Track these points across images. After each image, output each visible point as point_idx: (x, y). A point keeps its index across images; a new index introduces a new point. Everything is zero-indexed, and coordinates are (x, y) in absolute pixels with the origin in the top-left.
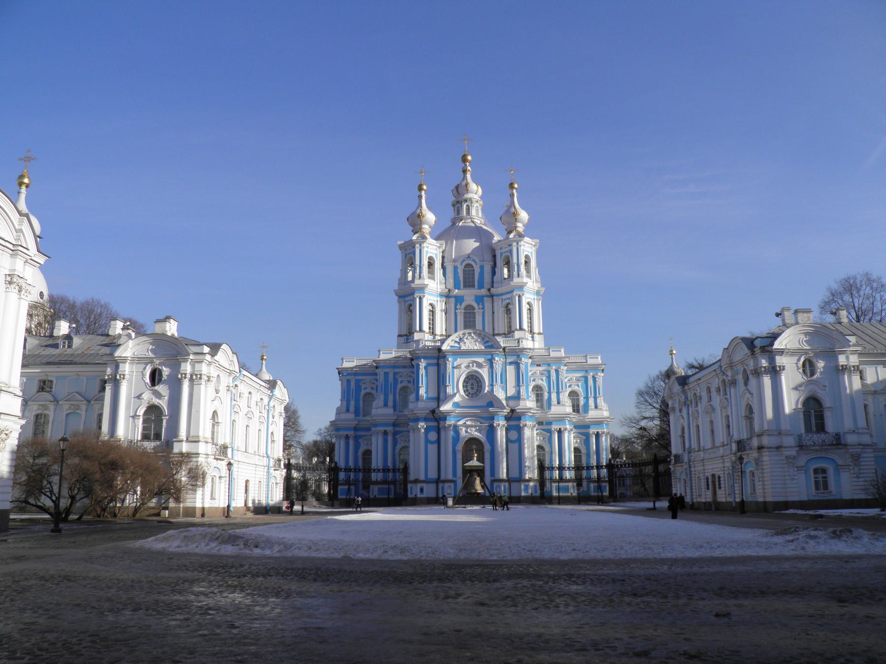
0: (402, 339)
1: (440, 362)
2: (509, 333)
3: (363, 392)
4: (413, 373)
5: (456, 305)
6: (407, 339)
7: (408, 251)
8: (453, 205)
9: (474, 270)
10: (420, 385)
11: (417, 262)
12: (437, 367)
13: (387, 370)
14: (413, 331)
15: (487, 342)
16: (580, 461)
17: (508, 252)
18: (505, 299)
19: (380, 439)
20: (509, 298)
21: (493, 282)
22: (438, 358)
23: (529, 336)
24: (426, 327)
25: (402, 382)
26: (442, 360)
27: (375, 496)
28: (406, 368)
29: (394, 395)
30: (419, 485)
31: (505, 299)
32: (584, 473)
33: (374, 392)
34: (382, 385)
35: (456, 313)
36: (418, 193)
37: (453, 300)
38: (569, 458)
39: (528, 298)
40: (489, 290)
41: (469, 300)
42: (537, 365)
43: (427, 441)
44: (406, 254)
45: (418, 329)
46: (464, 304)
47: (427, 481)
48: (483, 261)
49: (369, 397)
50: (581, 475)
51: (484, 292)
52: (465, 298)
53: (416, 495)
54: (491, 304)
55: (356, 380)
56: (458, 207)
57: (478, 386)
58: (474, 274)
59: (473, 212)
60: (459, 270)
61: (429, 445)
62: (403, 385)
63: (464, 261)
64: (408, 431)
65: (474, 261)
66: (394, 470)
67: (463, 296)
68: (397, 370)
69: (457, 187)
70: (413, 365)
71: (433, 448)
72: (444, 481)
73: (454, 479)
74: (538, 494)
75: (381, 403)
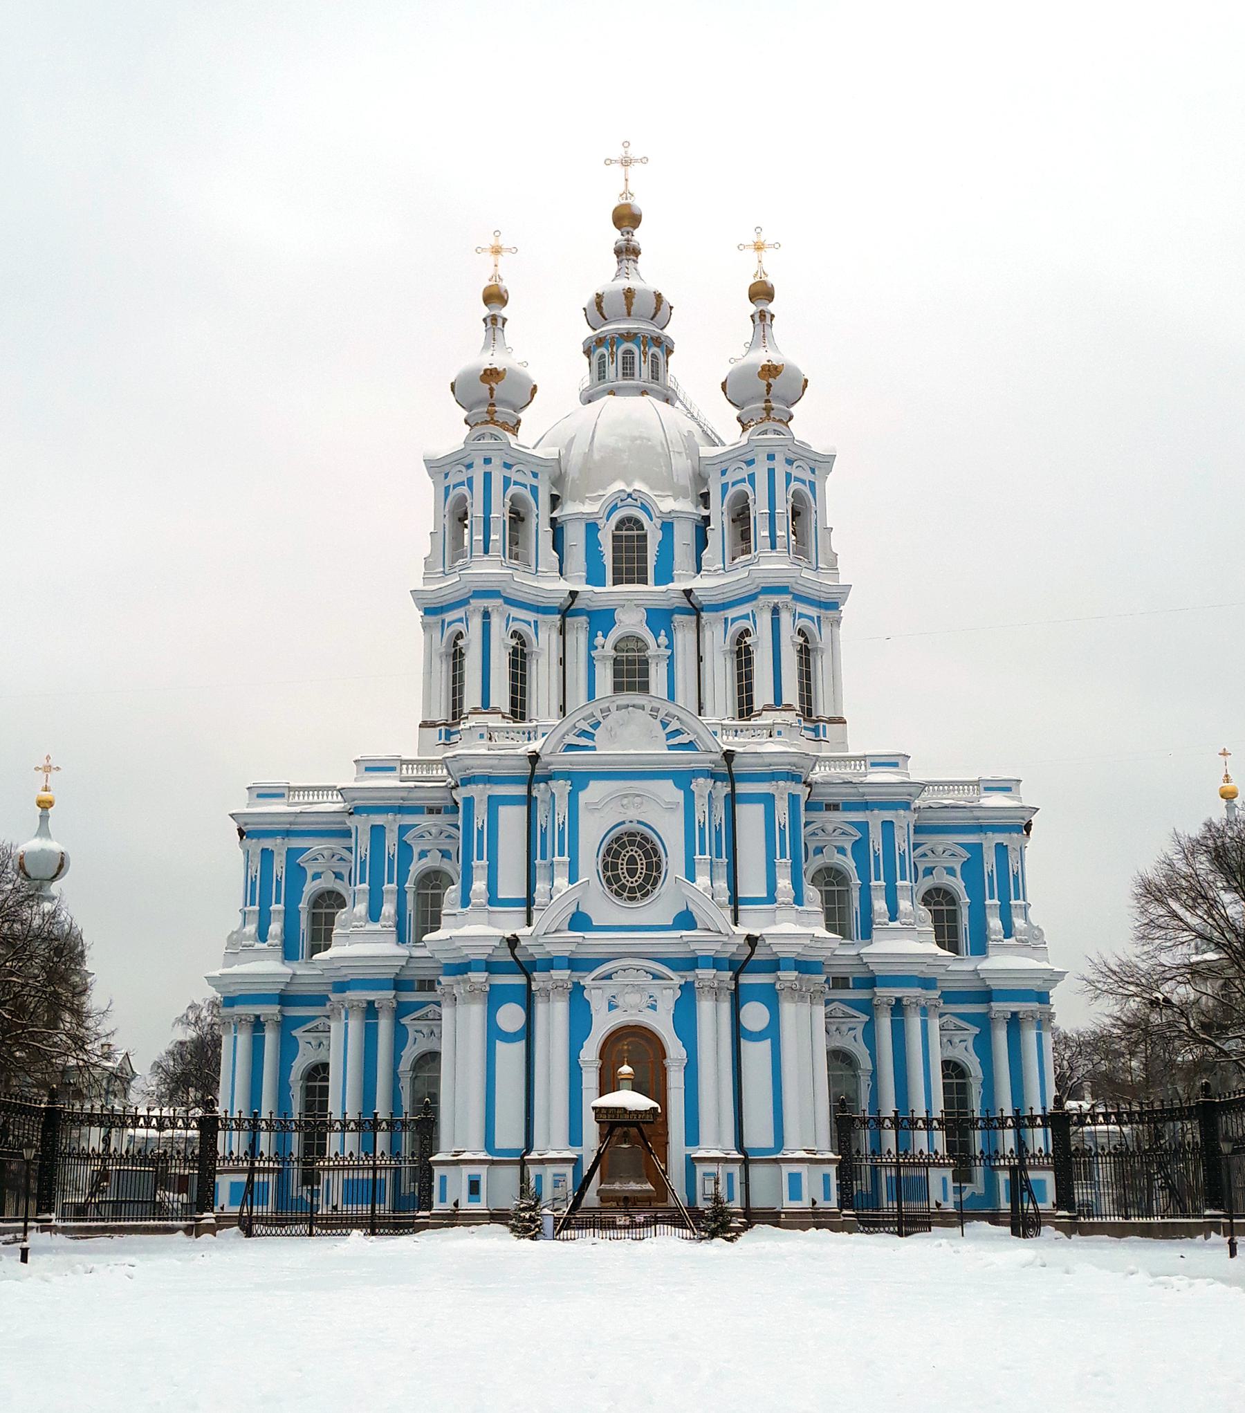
1: (534, 794)
5: (592, 637)
6: (449, 734)
7: (452, 480)
8: (588, 352)
10: (475, 863)
12: (525, 808)
13: (378, 820)
14: (466, 709)
15: (677, 732)
16: (964, 1102)
17: (743, 480)
18: (734, 620)
19: (355, 1025)
20: (746, 617)
22: (531, 780)
24: (501, 697)
26: (542, 785)
27: (335, 1208)
28: (439, 812)
29: (401, 894)
30: (467, 1171)
31: (734, 620)
32: (978, 1139)
33: (339, 886)
34: (363, 863)
37: (578, 624)
39: (801, 615)
41: (631, 622)
43: (494, 1034)
44: (447, 488)
49: (329, 902)
50: (966, 1146)
52: (619, 615)
53: (456, 1204)
56: (603, 356)
57: (649, 866)
64: (438, 1004)
65: (644, 508)
66: (393, 1125)
68: (408, 820)
69: (599, 297)
70: (456, 803)
71: (510, 1055)
74: (833, 1204)
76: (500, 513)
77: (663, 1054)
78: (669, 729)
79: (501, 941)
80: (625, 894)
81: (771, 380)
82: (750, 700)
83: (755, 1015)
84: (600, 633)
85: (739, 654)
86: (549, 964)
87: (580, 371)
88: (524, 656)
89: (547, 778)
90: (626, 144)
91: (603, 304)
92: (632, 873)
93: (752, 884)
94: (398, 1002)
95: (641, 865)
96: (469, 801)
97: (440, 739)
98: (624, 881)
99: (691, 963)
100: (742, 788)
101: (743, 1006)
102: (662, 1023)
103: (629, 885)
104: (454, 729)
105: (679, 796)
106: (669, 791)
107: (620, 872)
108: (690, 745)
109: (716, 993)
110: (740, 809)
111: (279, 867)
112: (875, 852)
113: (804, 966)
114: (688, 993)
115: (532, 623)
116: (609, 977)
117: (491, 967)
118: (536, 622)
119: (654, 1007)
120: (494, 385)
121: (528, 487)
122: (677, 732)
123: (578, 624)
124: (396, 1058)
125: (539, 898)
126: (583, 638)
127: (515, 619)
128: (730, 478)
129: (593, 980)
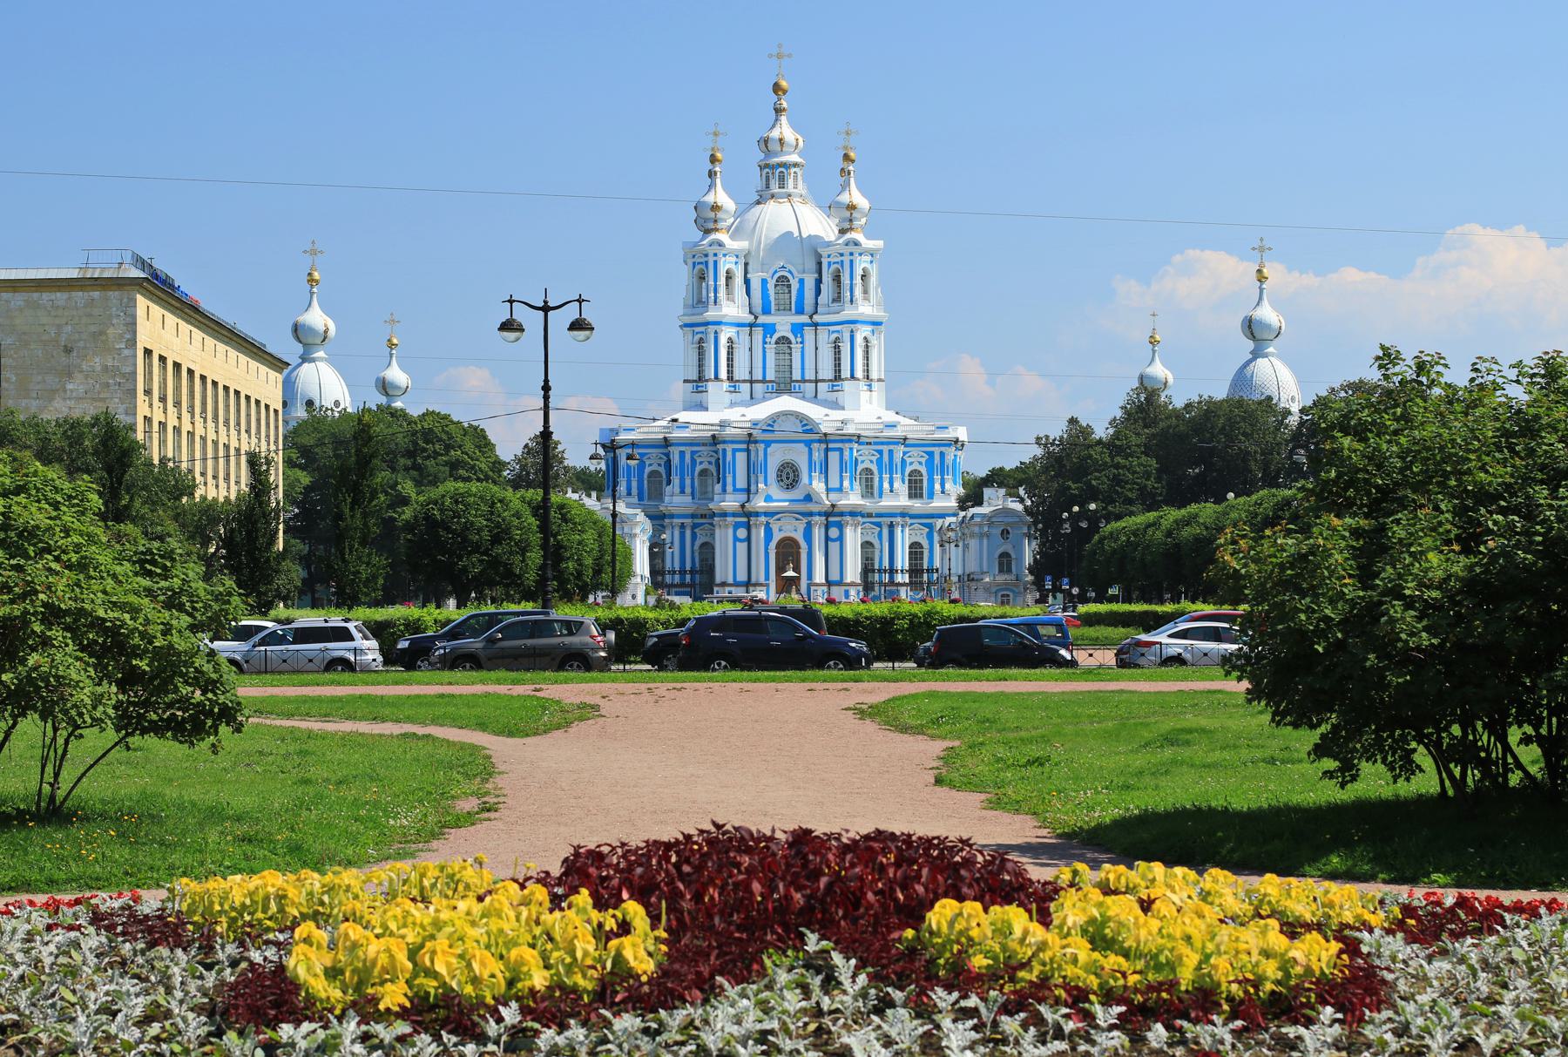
0: (690, 385)
2: (838, 377)
3: (647, 470)
5: (765, 337)
9: (789, 286)
11: (711, 283)
21: (817, 303)
22: (749, 443)
23: (862, 385)
24: (723, 374)
25: (701, 463)
29: (693, 479)
35: (764, 348)
36: (710, 166)
37: (758, 334)
38: (902, 560)
40: (811, 317)
41: (784, 330)
43: (736, 539)
46: (776, 336)
47: (736, 584)
48: (804, 272)
51: (804, 319)
52: (777, 327)
59: (791, 182)
62: (702, 467)
65: (790, 272)
66: (692, 572)
71: (742, 547)
75: (677, 490)
76: (722, 281)
83: (834, 533)
86: (757, 514)
87: (756, 181)
89: (756, 442)
90: (780, 46)
93: (834, 483)
95: (791, 475)
96: (724, 450)
99: (811, 514)
100: (831, 446)
102: (799, 537)
108: (810, 431)
113: (853, 514)
114: (809, 527)
117: (734, 515)
123: (758, 334)
125: (753, 488)
126: (760, 337)
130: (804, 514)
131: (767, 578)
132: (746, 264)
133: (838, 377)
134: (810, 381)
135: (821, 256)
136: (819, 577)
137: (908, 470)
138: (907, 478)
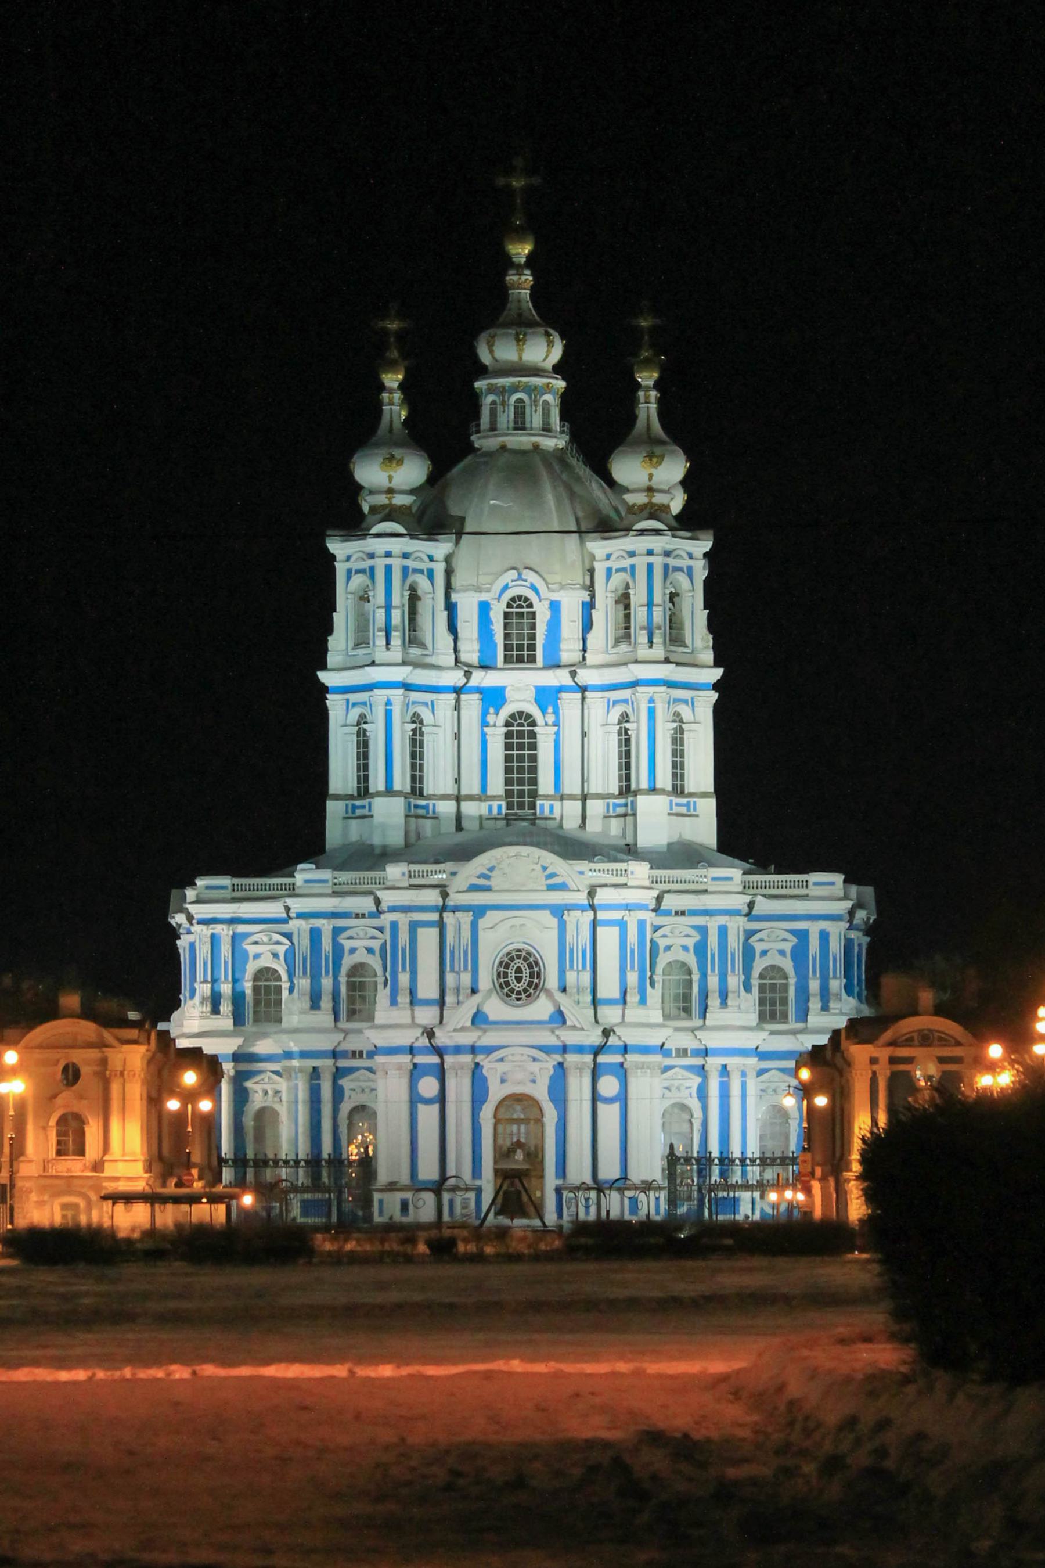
1: (445, 920)
4: (381, 930)
5: (485, 713)
9: (533, 615)
12: (438, 929)
14: (371, 790)
17: (622, 570)
18: (615, 703)
20: (626, 701)
30: (399, 1196)
31: (615, 703)
35: (484, 735)
37: (471, 703)
42: (677, 913)
43: (415, 1100)
45: (381, 787)
47: (418, 1187)
51: (561, 678)
52: (508, 694)
53: (391, 1218)
54: (580, 711)
55: (234, 937)
57: (532, 975)
58: (533, 627)
60: (492, 614)
61: (421, 1107)
63: (506, 588)
65: (533, 588)
67: (503, 689)
71: (428, 1115)
72: (454, 1189)
73: (478, 1183)
77: (542, 1115)
78: (548, 872)
79: (423, 1034)
80: (514, 996)
81: (653, 471)
82: (628, 778)
83: (609, 1085)
84: (492, 710)
85: (620, 734)
88: (422, 734)
89: (455, 910)
91: (494, 348)
92: (519, 980)
93: (608, 988)
94: (337, 1068)
95: (526, 973)
96: (394, 925)
97: (347, 812)
98: (512, 986)
101: (599, 1078)
102: (541, 1092)
103: (517, 989)
104: (358, 803)
105: (554, 922)
106: (547, 918)
107: (509, 979)
109: (581, 1070)
110: (599, 929)
111: (225, 950)
112: (711, 950)
115: (430, 703)
116: (502, 1060)
118: (432, 702)
119: (534, 1081)
120: (392, 473)
121: (425, 573)
122: (553, 875)
123: (471, 703)
124: (336, 1111)
125: (450, 999)
127: (414, 703)
128: (615, 564)
129: (490, 1062)
130: (546, 1050)
131: (477, 1172)
132: (449, 573)
133: (627, 790)
134: (572, 797)
135: (593, 557)
136: (579, 1171)
137: (759, 965)
138: (755, 982)
